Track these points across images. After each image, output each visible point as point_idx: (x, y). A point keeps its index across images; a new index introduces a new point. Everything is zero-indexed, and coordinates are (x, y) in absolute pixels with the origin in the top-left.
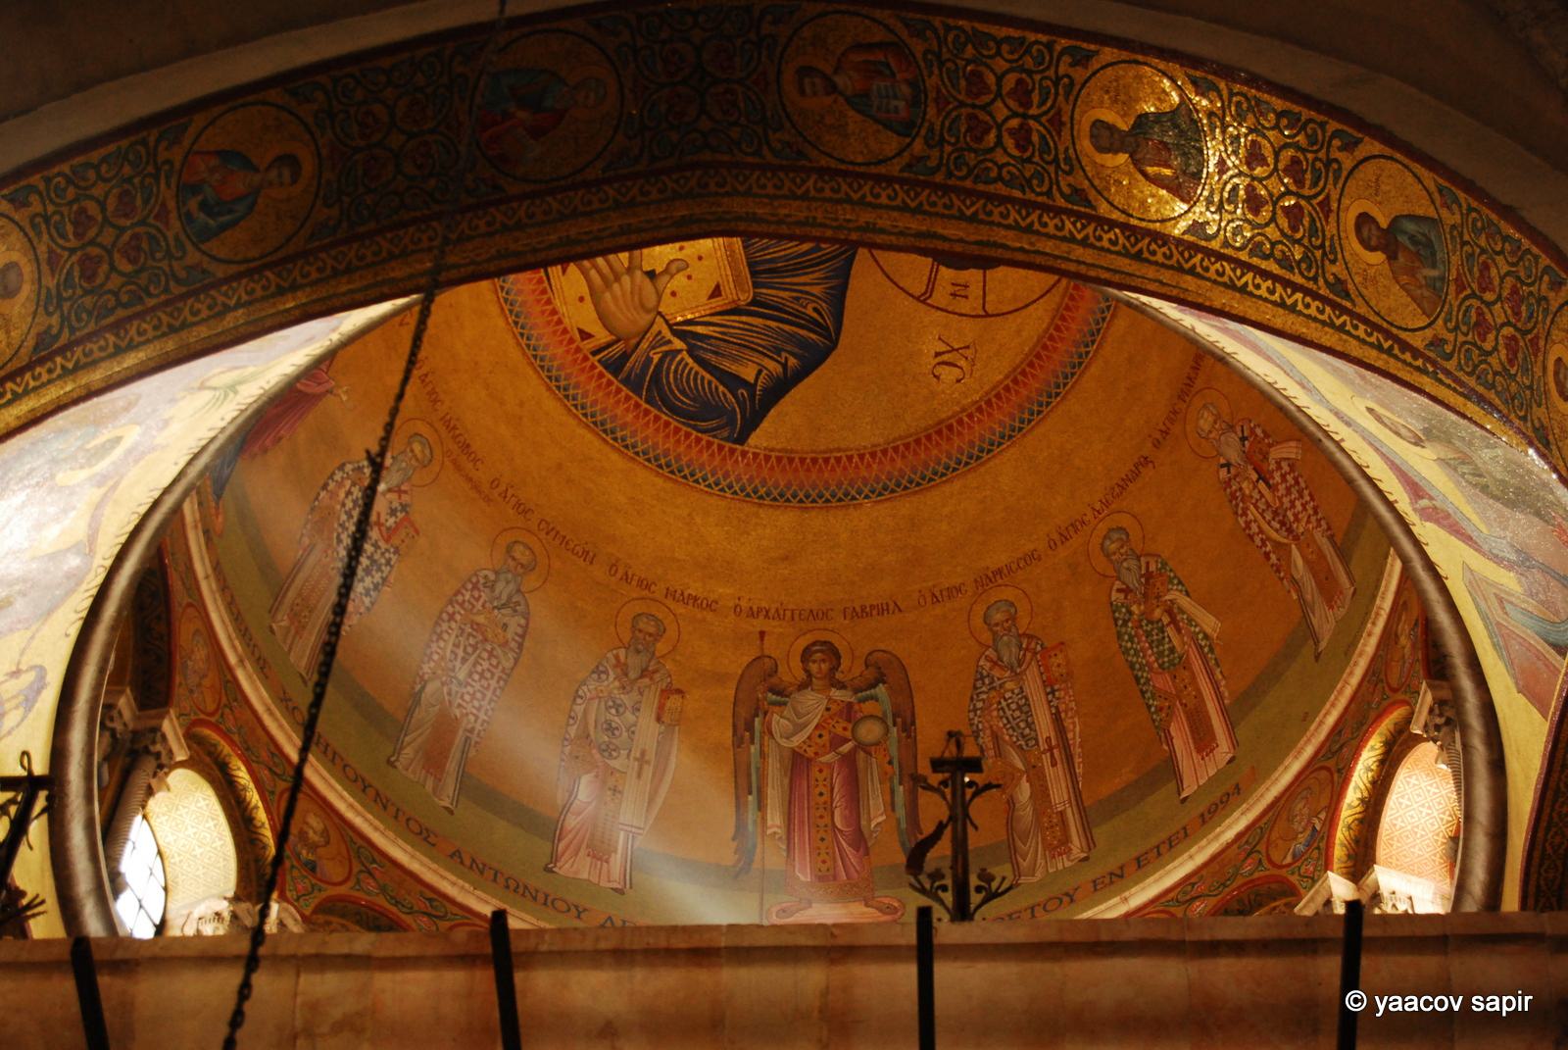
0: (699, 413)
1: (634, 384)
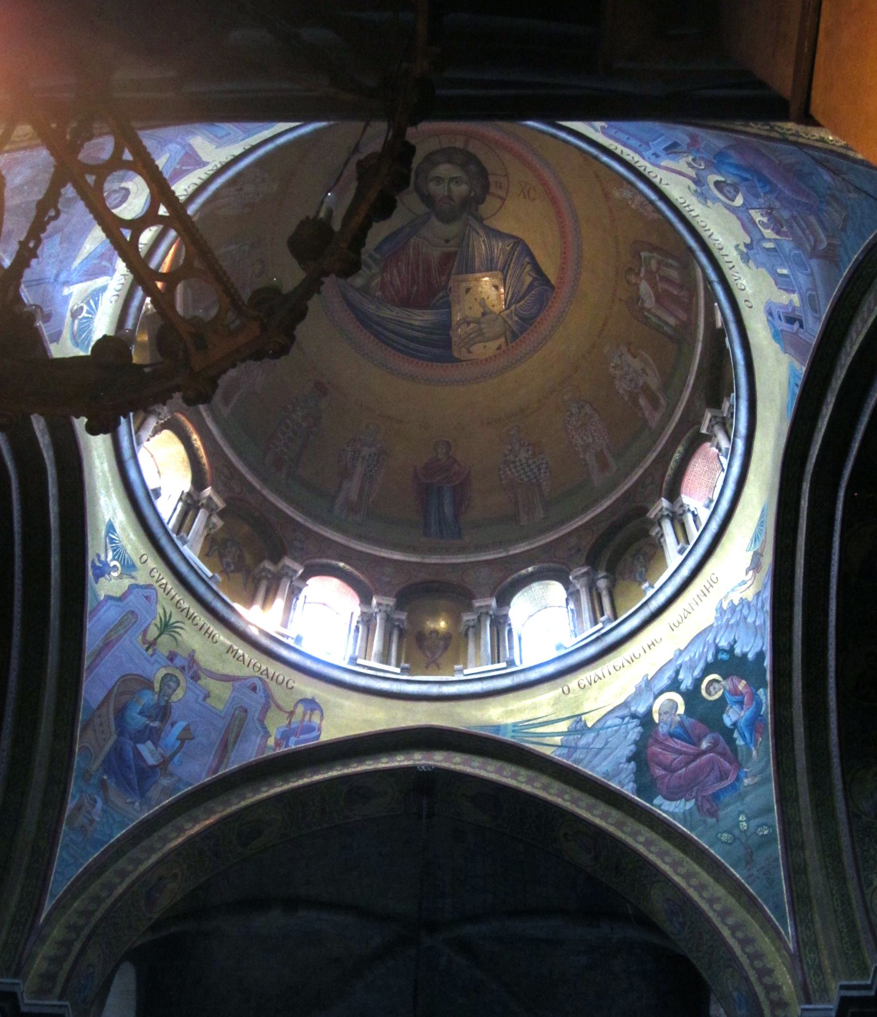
0: (542, 303)
1: (523, 330)
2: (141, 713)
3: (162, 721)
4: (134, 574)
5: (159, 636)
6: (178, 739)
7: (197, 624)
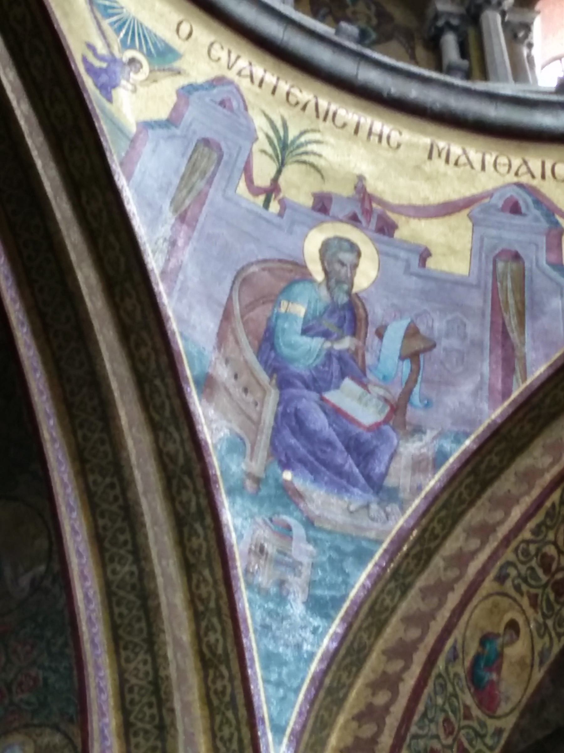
2: (305, 331)
3: (354, 333)
4: (177, 64)
5: (279, 172)
6: (402, 358)
7: (344, 125)
